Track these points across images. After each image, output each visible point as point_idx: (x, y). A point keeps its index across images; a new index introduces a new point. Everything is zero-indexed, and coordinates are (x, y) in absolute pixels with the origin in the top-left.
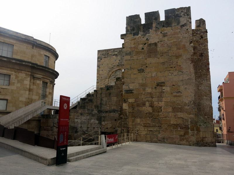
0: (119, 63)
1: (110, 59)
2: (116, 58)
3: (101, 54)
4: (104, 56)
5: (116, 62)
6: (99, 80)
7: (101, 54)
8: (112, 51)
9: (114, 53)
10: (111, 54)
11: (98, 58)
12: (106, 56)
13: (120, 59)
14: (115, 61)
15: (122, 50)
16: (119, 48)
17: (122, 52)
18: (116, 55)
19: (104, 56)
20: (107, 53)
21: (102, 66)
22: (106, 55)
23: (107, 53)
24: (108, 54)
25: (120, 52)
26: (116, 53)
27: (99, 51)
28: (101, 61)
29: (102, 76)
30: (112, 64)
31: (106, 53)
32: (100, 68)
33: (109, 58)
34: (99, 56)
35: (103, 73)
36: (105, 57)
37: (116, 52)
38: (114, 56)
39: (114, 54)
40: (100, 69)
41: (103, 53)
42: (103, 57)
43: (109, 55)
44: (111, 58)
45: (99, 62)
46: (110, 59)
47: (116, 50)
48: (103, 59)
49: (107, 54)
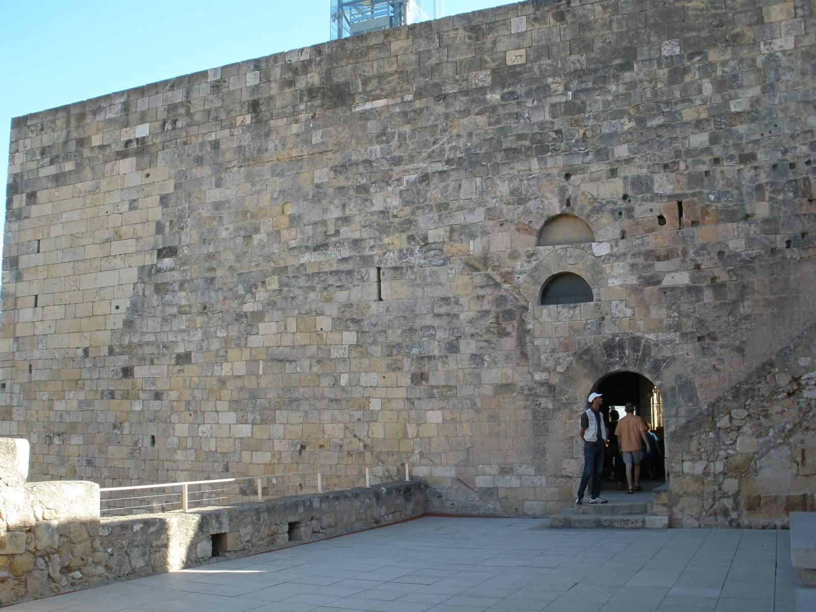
0: (159, 228)
1: (92, 192)
2: (136, 179)
3: (30, 153)
4: (52, 163)
5: (136, 215)
6: (17, 389)
7: (30, 153)
8: (114, 112)
9: (126, 135)
10: (102, 147)
11: (13, 189)
12: (69, 166)
13: (170, 188)
14: (133, 205)
15: (187, 103)
16: (165, 83)
17: (188, 114)
18: (141, 150)
19: (52, 170)
20: (74, 135)
21: (39, 259)
22: (67, 158)
23: (74, 135)
24: (81, 142)
25: (175, 122)
26: (142, 131)
27: (19, 123)
28: (35, 210)
29: (36, 354)
30: (106, 235)
31: (66, 143)
32: (18, 278)
33: (88, 185)
34: (17, 169)
35: (40, 328)
36: (58, 179)
37: (143, 119)
38: (127, 165)
39: (128, 142)
40: (22, 289)
41: (46, 139)
42: (44, 172)
43: (86, 153)
44: (104, 182)
45: (15, 226)
46: (92, 192)
47: (142, 104)
48: (42, 195)
49: (72, 146)
